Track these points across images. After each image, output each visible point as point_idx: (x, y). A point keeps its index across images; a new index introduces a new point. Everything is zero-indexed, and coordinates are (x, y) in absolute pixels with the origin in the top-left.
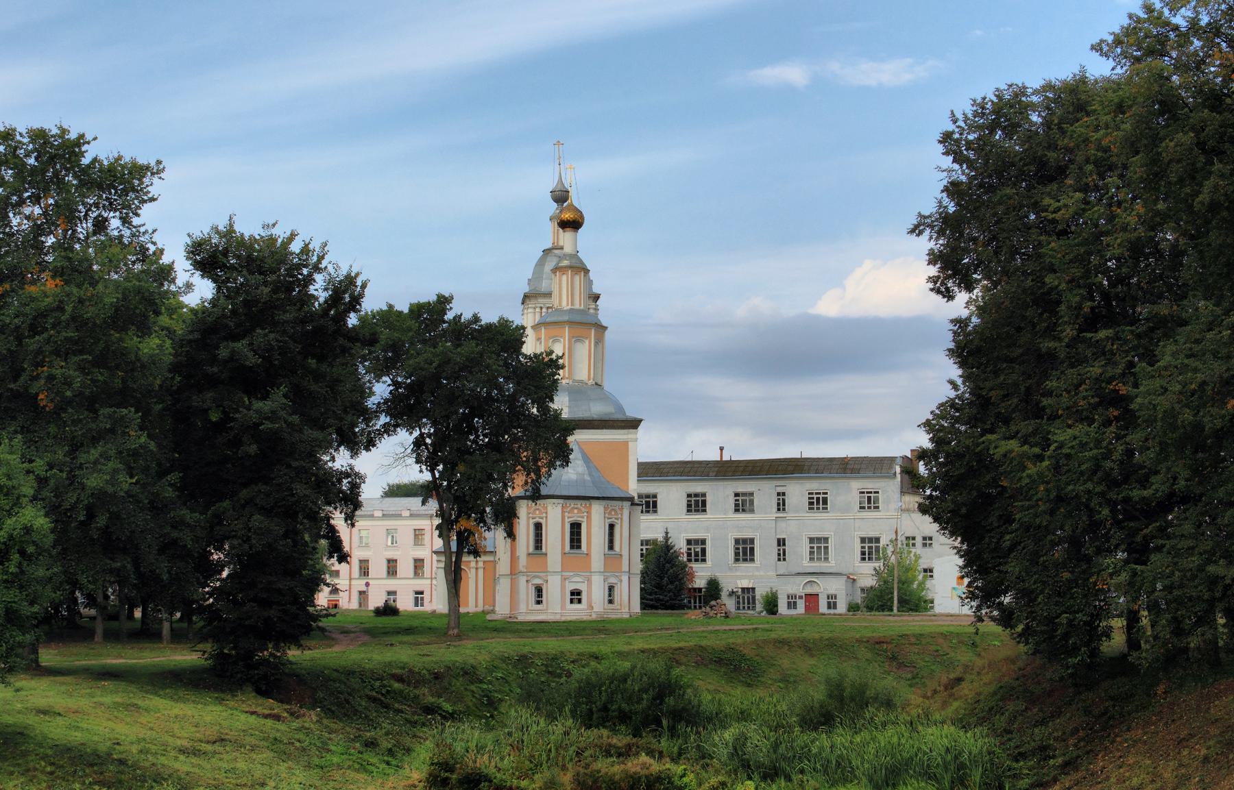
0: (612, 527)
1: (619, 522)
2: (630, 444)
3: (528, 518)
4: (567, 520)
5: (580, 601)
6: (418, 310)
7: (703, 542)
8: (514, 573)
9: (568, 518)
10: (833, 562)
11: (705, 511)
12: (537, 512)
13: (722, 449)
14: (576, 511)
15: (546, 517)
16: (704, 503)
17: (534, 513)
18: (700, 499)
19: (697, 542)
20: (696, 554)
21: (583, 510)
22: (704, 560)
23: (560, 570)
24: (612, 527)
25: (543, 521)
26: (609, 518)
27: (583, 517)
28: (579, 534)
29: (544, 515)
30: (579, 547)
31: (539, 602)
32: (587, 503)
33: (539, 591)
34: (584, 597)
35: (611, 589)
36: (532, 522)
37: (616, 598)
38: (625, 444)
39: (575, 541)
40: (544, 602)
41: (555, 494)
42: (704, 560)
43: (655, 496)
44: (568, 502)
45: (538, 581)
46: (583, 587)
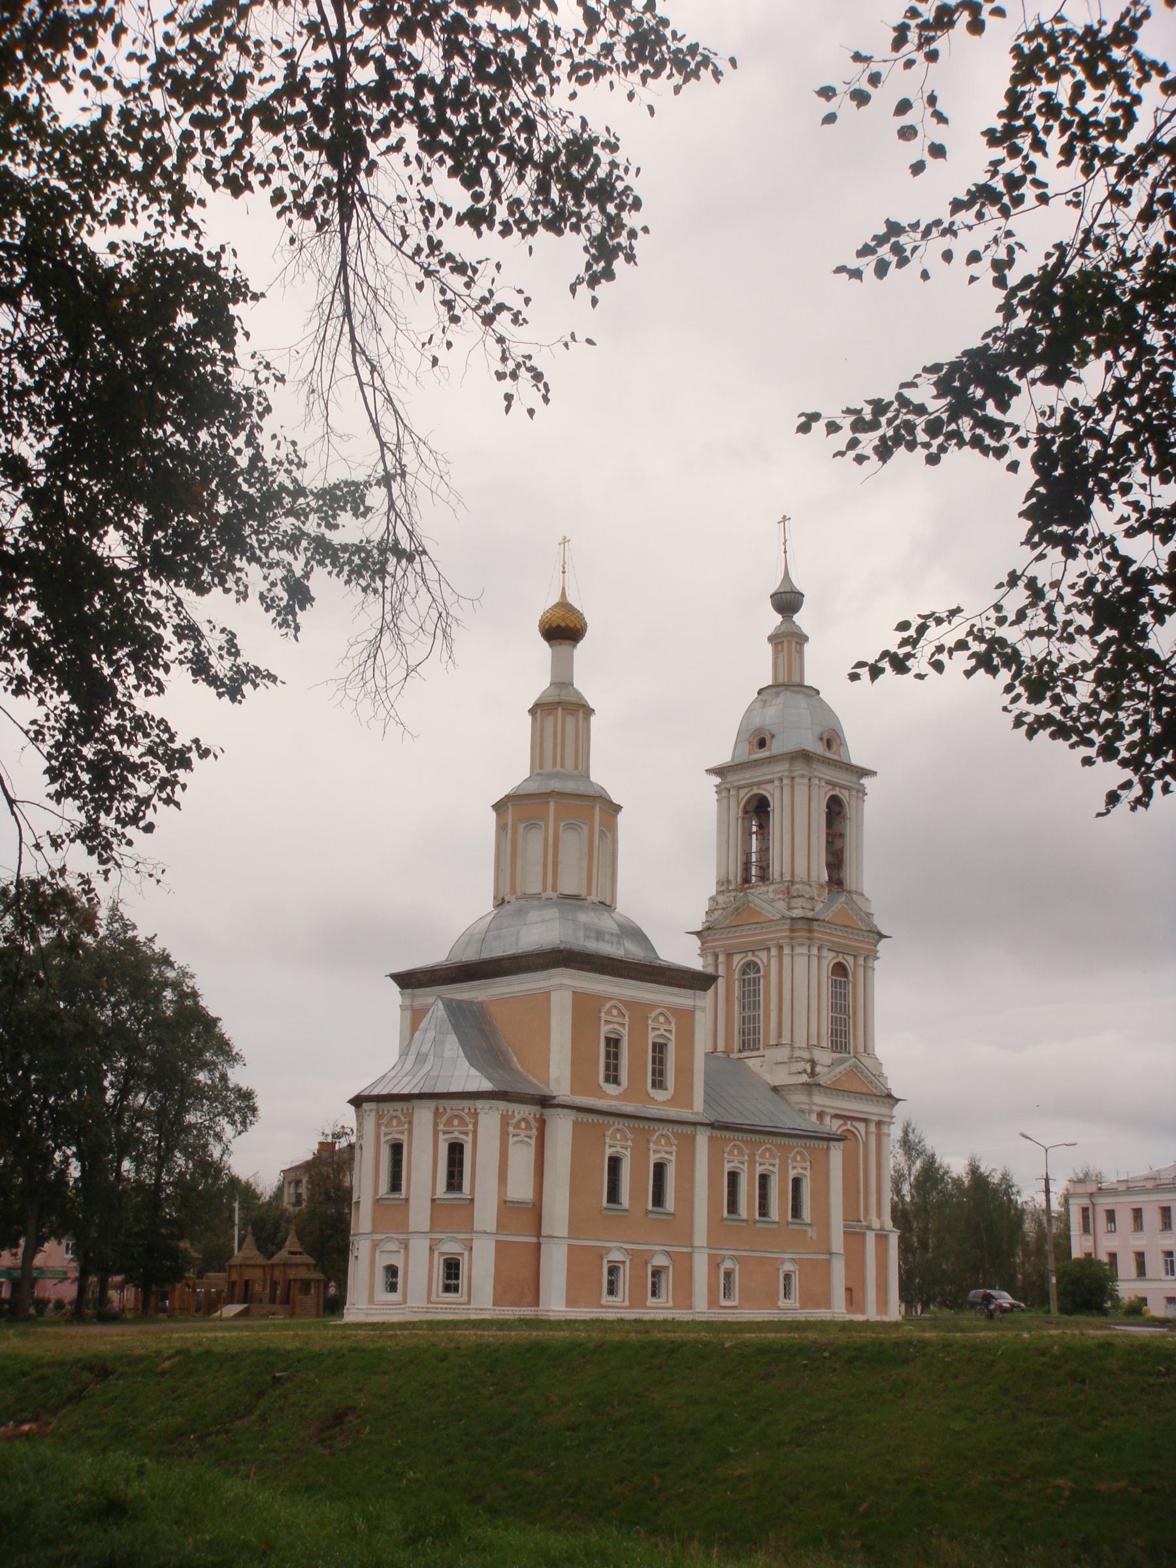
1: (469, 1139)
4: (383, 1139)
9: (386, 1134)
23: (427, 1229)
24: (456, 1150)
26: (445, 1133)
31: (392, 1287)
37: (463, 1282)
40: (400, 1286)
41: (436, 1091)
46: (398, 1261)
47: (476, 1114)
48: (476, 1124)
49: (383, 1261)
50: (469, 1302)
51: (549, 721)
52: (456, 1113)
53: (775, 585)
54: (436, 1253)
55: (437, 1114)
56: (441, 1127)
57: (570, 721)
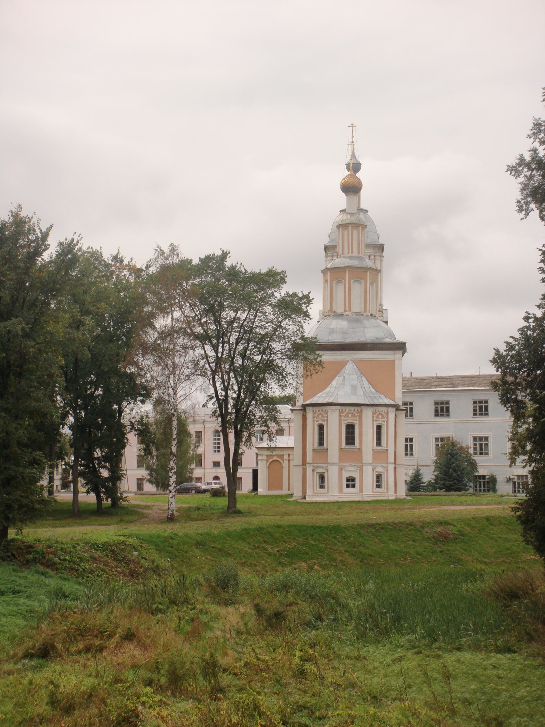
0: (379, 428)
1: (385, 424)
2: (397, 362)
3: (314, 421)
4: (343, 422)
5: (354, 486)
6: (207, 260)
8: (304, 463)
9: (344, 420)
10: (492, 456)
11: (487, 414)
12: (320, 416)
14: (350, 415)
15: (327, 420)
16: (487, 408)
17: (318, 417)
18: (483, 405)
21: (356, 414)
23: (338, 462)
24: (379, 428)
25: (325, 424)
26: (376, 421)
27: (356, 420)
28: (353, 433)
29: (325, 418)
30: (353, 444)
31: (322, 487)
32: (359, 409)
33: (322, 478)
34: (357, 483)
35: (379, 477)
36: (316, 423)
37: (384, 484)
38: (392, 362)
39: (350, 439)
40: (326, 487)
43: (448, 403)
44: (344, 408)
45: (321, 470)
47: (388, 413)
48: (387, 418)
49: (346, 475)
50: (387, 492)
51: (346, 232)
52: (381, 412)
53: (348, 159)
54: (375, 472)
55: (374, 413)
56: (375, 418)
57: (355, 232)
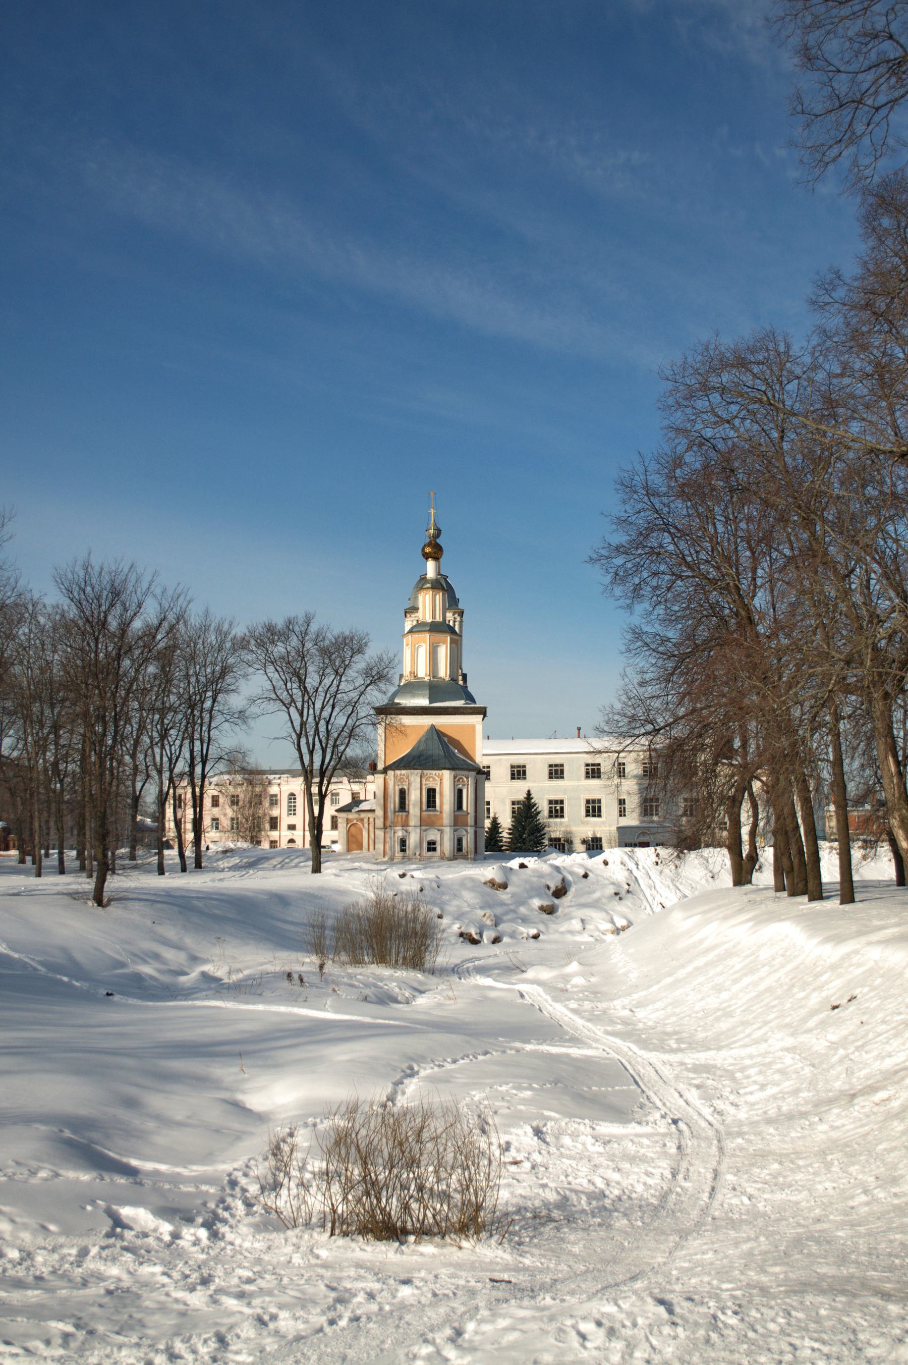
4: (424, 787)
7: (562, 802)
11: (563, 778)
13: (579, 729)
16: (562, 772)
19: (556, 802)
20: (556, 811)
22: (562, 816)
24: (460, 792)
30: (435, 806)
36: (397, 788)
42: (562, 816)
